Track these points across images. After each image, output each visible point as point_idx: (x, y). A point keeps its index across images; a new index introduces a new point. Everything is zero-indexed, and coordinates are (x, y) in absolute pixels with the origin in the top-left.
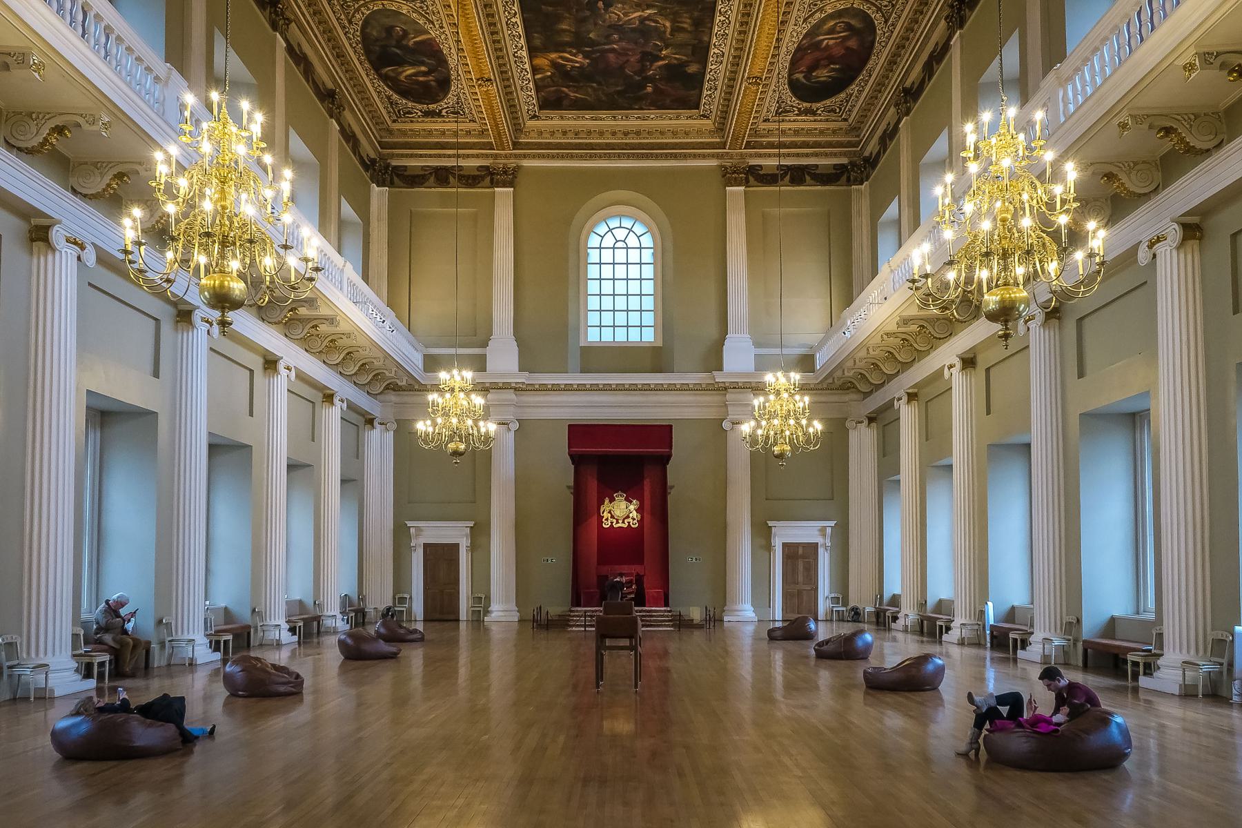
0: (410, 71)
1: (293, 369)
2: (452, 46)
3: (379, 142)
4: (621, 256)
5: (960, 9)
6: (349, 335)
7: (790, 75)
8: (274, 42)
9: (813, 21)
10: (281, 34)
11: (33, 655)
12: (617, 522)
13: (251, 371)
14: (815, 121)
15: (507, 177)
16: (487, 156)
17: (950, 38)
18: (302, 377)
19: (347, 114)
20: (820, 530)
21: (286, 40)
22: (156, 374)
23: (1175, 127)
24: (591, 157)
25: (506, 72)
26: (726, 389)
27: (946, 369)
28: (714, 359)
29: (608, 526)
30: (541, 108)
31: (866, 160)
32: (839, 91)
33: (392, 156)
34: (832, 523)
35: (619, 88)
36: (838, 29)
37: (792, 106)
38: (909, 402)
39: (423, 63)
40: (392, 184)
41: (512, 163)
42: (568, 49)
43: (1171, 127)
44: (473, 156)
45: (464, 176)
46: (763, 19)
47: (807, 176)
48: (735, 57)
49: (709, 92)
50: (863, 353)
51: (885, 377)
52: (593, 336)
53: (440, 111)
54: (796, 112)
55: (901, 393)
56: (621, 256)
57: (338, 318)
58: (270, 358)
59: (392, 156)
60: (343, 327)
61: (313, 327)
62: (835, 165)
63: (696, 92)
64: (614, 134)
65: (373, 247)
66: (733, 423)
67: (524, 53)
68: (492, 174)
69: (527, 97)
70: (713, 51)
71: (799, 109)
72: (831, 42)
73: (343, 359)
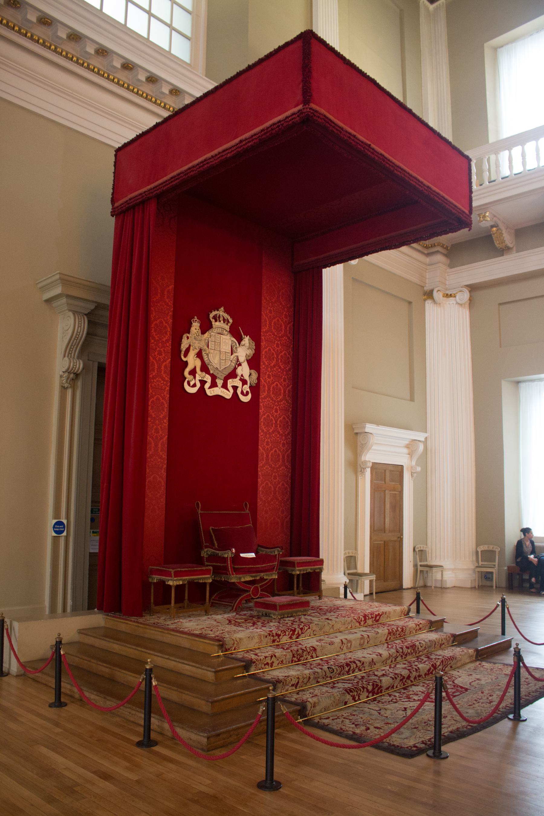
12: (214, 385)
29: (193, 390)
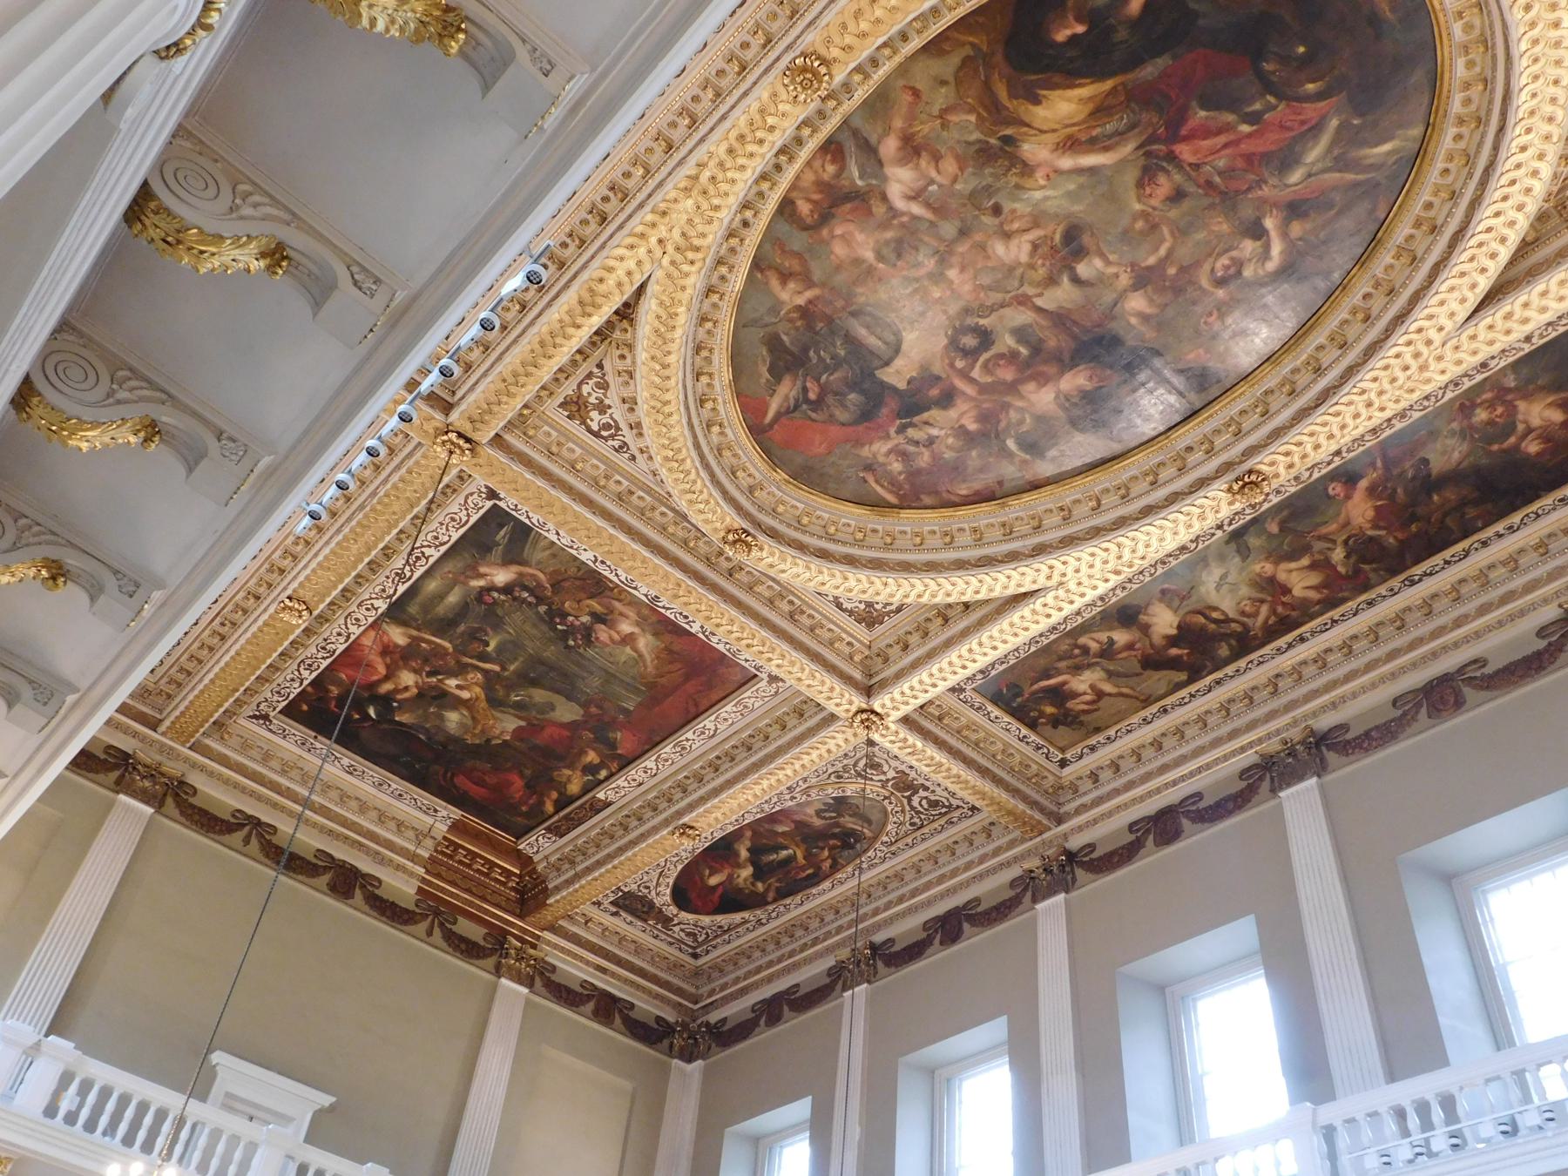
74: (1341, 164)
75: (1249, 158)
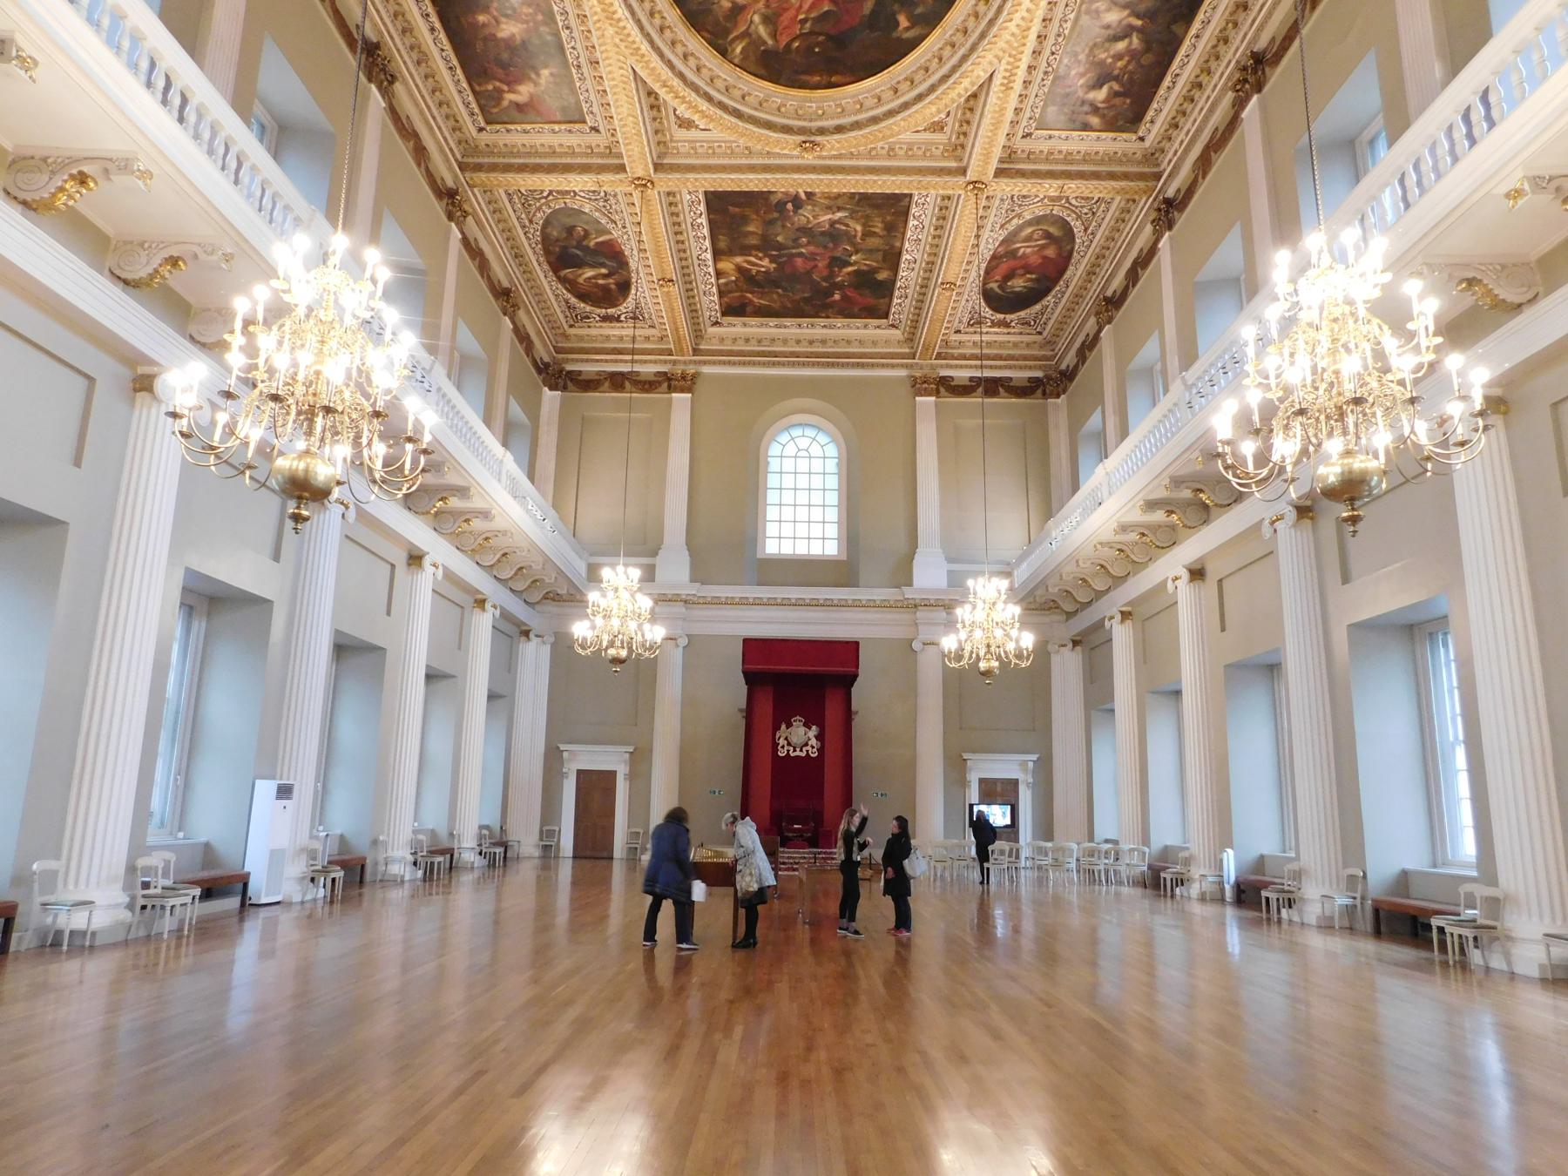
0: (589, 273)
1: (440, 567)
2: (634, 248)
3: (554, 347)
4: (803, 465)
5: (1167, 212)
6: (505, 533)
7: (984, 284)
8: (448, 232)
9: (1011, 227)
10: (457, 224)
11: (71, 887)
12: (795, 751)
13: (393, 566)
14: (1008, 333)
15: (685, 383)
16: (665, 362)
17: (1157, 241)
18: (449, 576)
19: (521, 314)
20: (1020, 765)
21: (462, 233)
22: (276, 557)
23: (1479, 277)
24: (774, 364)
25: (689, 275)
26: (916, 606)
27: (1170, 582)
28: (903, 573)
30: (724, 314)
31: (1063, 373)
32: (1035, 302)
33: (567, 361)
34: (1034, 757)
35: (806, 295)
36: (1035, 236)
37: (985, 318)
38: (1122, 621)
39: (603, 265)
40: (565, 389)
41: (691, 370)
42: (754, 253)
43: (1474, 278)
44: (651, 361)
45: (640, 382)
46: (959, 221)
47: (1001, 389)
48: (928, 263)
49: (899, 301)
50: (1070, 568)
51: (1093, 596)
52: (772, 548)
53: (619, 316)
54: (989, 324)
55: (1115, 611)
56: (803, 465)
57: (493, 512)
58: (415, 553)
59: (567, 361)
60: (498, 523)
61: (465, 521)
62: (1030, 378)
63: (887, 300)
64: (798, 342)
65: (541, 451)
66: (924, 644)
67: (709, 256)
68: (669, 379)
69: (710, 302)
70: (905, 257)
71: (992, 321)
72: (1029, 250)
73: (499, 561)
74: (746, 34)
75: (785, 10)
